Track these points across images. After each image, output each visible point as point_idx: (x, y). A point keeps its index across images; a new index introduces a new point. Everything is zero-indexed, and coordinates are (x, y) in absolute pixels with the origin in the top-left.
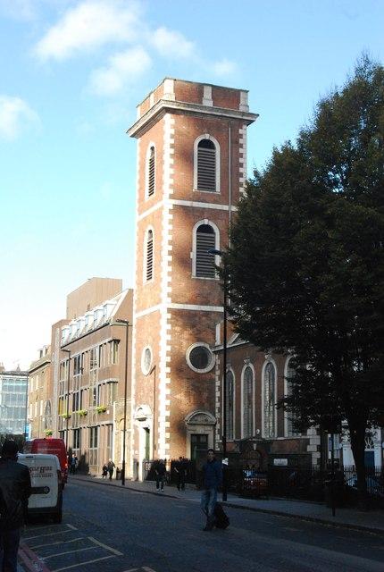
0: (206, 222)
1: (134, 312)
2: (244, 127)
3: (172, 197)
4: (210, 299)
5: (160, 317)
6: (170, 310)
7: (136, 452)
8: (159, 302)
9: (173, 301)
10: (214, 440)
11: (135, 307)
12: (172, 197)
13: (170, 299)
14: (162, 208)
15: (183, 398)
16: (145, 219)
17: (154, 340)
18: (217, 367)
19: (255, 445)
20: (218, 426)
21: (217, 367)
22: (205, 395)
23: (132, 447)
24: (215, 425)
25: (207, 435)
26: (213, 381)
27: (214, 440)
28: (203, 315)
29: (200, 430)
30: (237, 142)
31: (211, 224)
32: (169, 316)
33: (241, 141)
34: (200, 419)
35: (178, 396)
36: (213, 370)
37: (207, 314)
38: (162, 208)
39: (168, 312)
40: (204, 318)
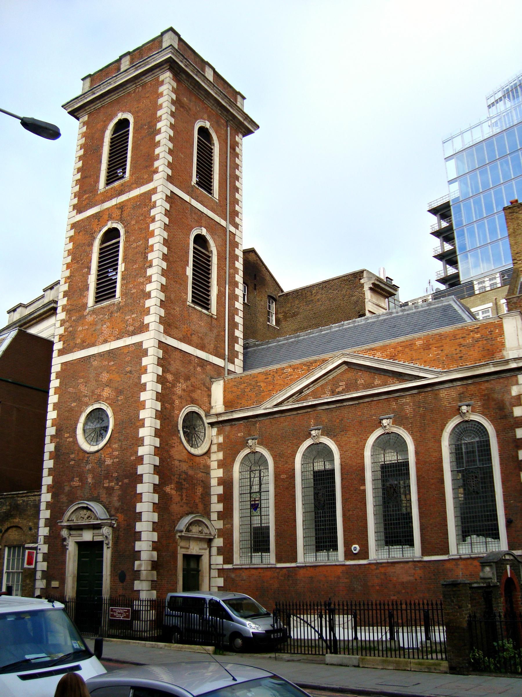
0: (204, 232)
1: (55, 354)
2: (240, 136)
3: (170, 179)
4: (206, 341)
5: (145, 353)
6: (161, 345)
7: (55, 584)
8: (143, 328)
9: (166, 332)
10: (210, 565)
11: (58, 346)
12: (170, 179)
13: (161, 328)
14: (154, 191)
15: (174, 492)
16: (97, 216)
17: (119, 392)
18: (214, 448)
19: (508, 567)
20: (219, 542)
21: (214, 448)
22: (199, 490)
23: (39, 575)
24: (210, 541)
25: (198, 558)
26: (207, 470)
27: (210, 565)
28: (198, 365)
29: (194, 549)
30: (234, 150)
31: (208, 237)
32: (160, 353)
33: (237, 150)
34: (195, 529)
35: (168, 489)
36: (208, 453)
37: (203, 363)
38: (154, 191)
39: (159, 348)
40: (199, 369)
